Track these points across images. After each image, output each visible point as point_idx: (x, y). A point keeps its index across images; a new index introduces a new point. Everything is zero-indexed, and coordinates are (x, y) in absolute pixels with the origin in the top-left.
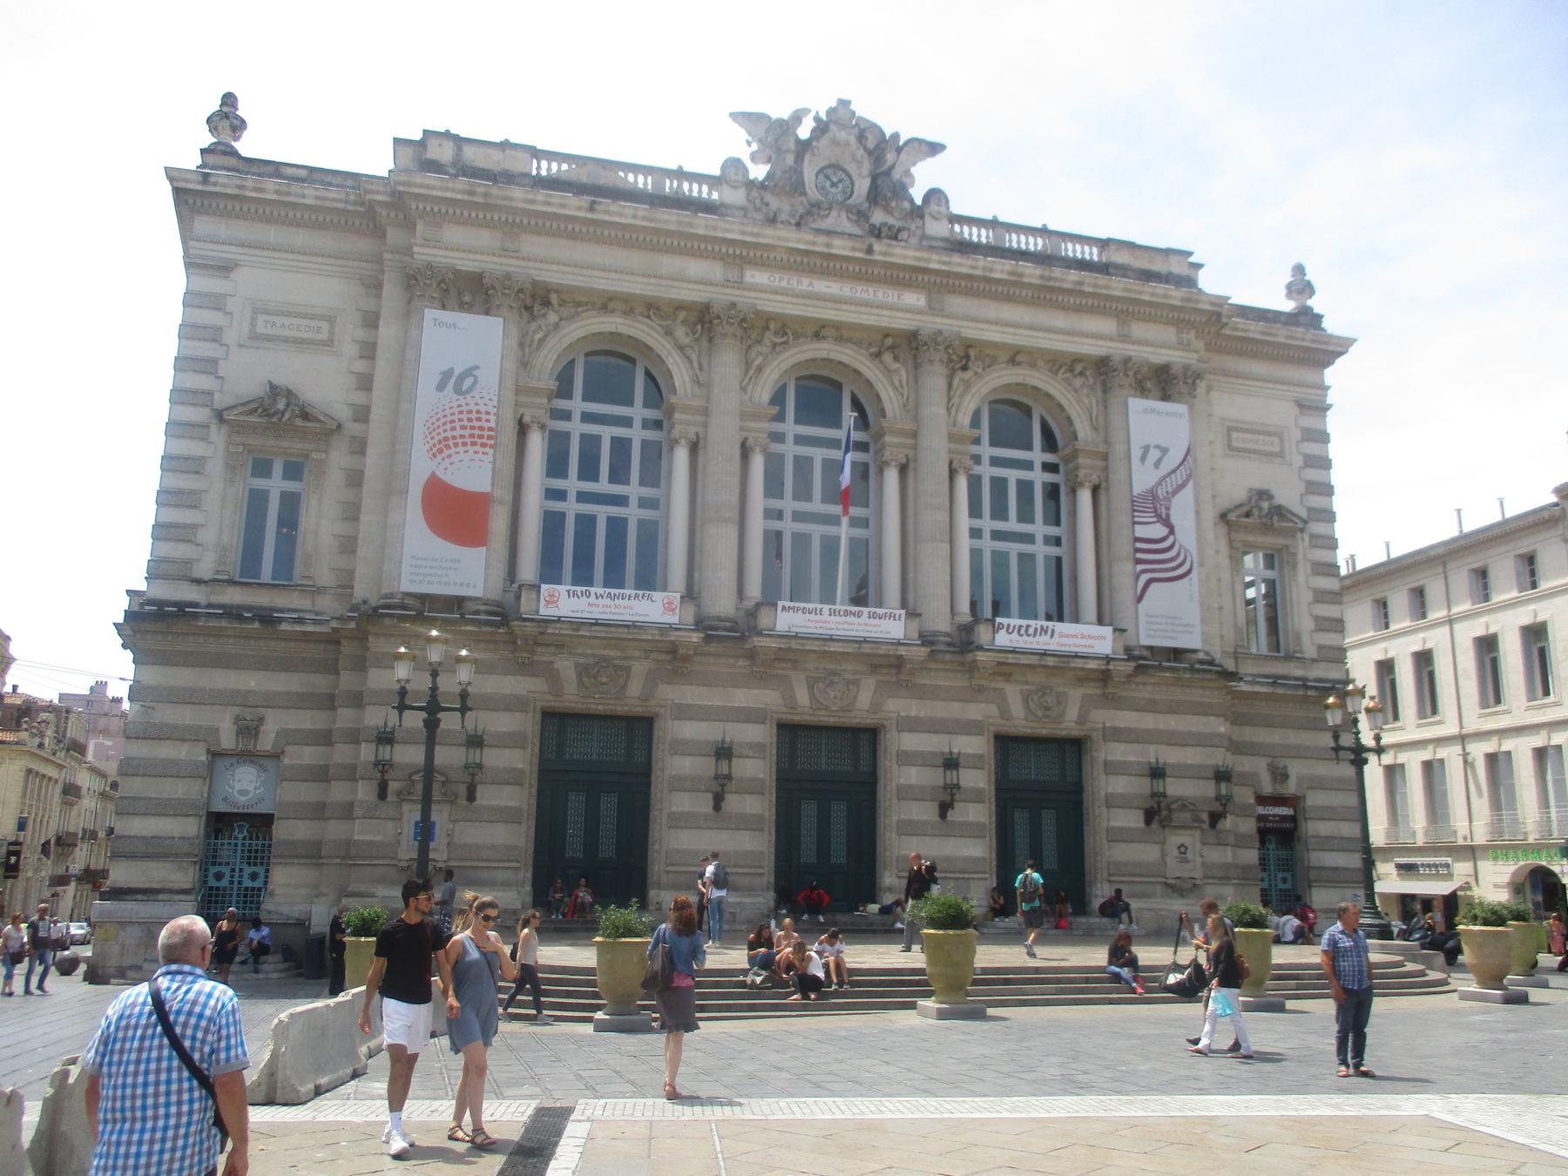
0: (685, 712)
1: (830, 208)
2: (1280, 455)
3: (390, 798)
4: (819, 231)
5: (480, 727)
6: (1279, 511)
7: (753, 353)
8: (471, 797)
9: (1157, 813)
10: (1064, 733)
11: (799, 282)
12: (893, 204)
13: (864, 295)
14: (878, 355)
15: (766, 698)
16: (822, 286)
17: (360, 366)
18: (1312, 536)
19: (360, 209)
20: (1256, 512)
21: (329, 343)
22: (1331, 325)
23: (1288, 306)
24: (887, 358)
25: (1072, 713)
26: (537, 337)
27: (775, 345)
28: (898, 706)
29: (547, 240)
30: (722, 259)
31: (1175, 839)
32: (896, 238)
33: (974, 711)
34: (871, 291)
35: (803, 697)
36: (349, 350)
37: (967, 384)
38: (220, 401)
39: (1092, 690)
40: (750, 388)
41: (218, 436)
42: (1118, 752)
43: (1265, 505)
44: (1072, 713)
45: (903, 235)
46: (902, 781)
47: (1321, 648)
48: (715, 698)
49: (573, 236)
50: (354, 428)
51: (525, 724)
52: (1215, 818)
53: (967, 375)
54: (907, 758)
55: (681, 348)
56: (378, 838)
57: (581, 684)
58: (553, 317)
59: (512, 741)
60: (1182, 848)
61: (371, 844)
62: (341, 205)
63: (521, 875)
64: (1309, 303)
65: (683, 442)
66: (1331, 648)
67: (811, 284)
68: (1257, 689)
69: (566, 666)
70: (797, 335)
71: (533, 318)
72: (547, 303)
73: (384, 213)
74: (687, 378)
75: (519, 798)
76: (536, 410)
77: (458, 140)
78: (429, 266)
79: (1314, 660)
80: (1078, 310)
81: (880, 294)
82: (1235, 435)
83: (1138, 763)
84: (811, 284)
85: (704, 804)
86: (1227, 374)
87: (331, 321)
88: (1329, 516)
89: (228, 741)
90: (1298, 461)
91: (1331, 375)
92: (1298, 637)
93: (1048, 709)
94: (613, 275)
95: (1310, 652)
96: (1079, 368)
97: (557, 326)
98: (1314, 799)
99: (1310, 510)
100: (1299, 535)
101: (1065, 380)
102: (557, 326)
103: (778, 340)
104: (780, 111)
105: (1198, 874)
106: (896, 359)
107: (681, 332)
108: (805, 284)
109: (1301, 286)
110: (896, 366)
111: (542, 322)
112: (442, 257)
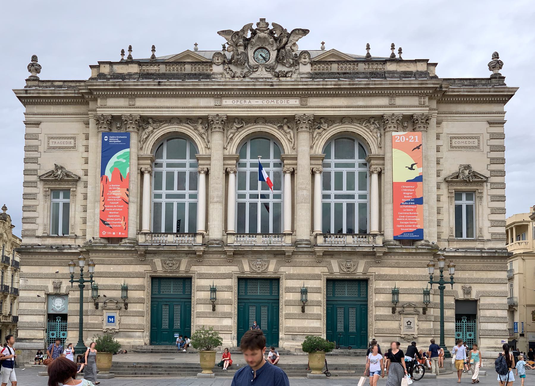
0: (202, 276)
1: (258, 68)
2: (478, 147)
3: (100, 308)
4: (252, 78)
5: (126, 284)
6: (475, 175)
7: (229, 133)
8: (126, 308)
9: (396, 308)
10: (357, 277)
11: (245, 102)
12: (285, 61)
13: (272, 103)
14: (281, 127)
15: (233, 269)
16: (254, 102)
18: (492, 183)
19: (79, 95)
20: (461, 176)
22: (509, 83)
23: (488, 74)
24: (285, 128)
25: (360, 269)
26: (144, 137)
27: (238, 128)
28: (285, 270)
29: (146, 99)
30: (213, 97)
31: (404, 320)
32: (286, 77)
33: (317, 270)
34: (275, 101)
35: (247, 268)
39: (369, 260)
40: (228, 148)
42: (381, 285)
43: (467, 172)
44: (360, 269)
45: (290, 75)
46: (286, 298)
47: (493, 234)
48: (213, 270)
49: (155, 96)
51: (146, 282)
52: (425, 310)
53: (319, 131)
54: (289, 290)
55: (201, 135)
56: (96, 322)
57: (163, 266)
58: (150, 128)
59: (141, 288)
60: (409, 323)
61: (94, 324)
62: (73, 95)
63: (145, 334)
64: (500, 71)
65: (202, 172)
67: (250, 102)
68: (457, 254)
70: (247, 123)
71: (144, 129)
72: (149, 123)
73: (87, 97)
74: (203, 147)
75: (144, 308)
76: (146, 165)
77: (111, 63)
78: (102, 115)
79: (489, 240)
81: (279, 101)
82: (454, 140)
83: (389, 289)
84: (250, 102)
85: (209, 309)
88: (502, 173)
90: (488, 149)
91: (507, 107)
92: (481, 229)
93: (349, 268)
94: (171, 109)
95: (487, 236)
96: (372, 121)
97: (152, 132)
98: (483, 301)
99: (491, 171)
100: (485, 184)
101: (366, 127)
102: (152, 132)
103: (238, 126)
104: (237, 28)
105: (416, 333)
106: (289, 127)
107: (200, 128)
108: (248, 102)
109: (496, 63)
110: (288, 130)
111: (147, 131)
112: (108, 112)
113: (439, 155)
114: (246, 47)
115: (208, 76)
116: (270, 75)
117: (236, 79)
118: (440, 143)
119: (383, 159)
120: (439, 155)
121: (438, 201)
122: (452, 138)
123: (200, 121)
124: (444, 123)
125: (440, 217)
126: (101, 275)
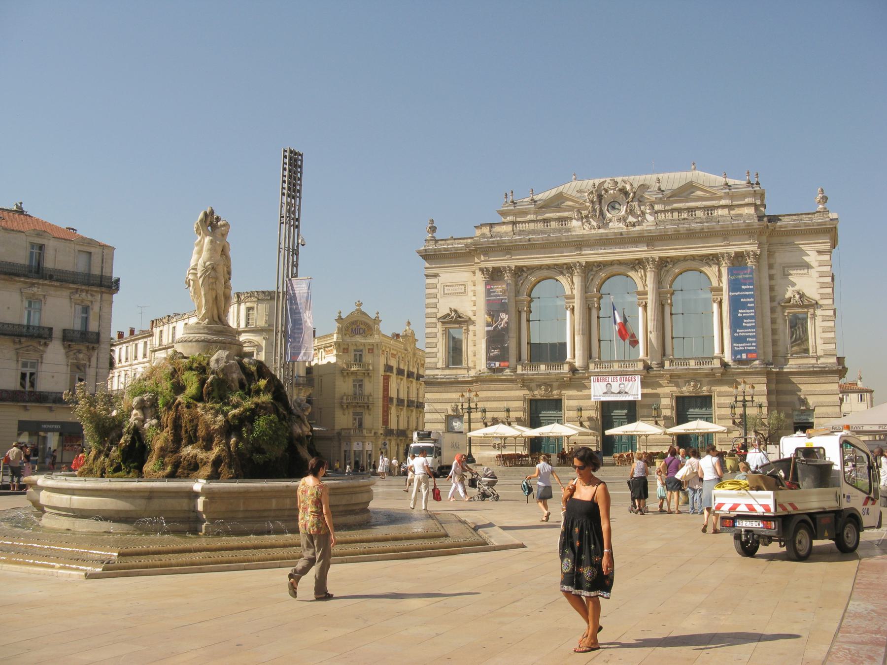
17: (474, 298)
21: (465, 292)
36: (471, 294)
37: (668, 271)
38: (439, 316)
41: (439, 325)
49: (526, 249)
50: (473, 318)
58: (525, 275)
66: (830, 350)
69: (533, 385)
79: (821, 356)
80: (706, 237)
86: (782, 244)
87: (464, 285)
89: (450, 412)
90: (817, 275)
112: (490, 265)
113: (773, 282)
114: (600, 203)
115: (568, 230)
116: (621, 225)
117: (593, 231)
118: (773, 272)
119: (722, 290)
120: (773, 282)
121: (773, 321)
122: (784, 267)
123: (565, 267)
124: (777, 254)
125: (777, 337)
126: (488, 400)
